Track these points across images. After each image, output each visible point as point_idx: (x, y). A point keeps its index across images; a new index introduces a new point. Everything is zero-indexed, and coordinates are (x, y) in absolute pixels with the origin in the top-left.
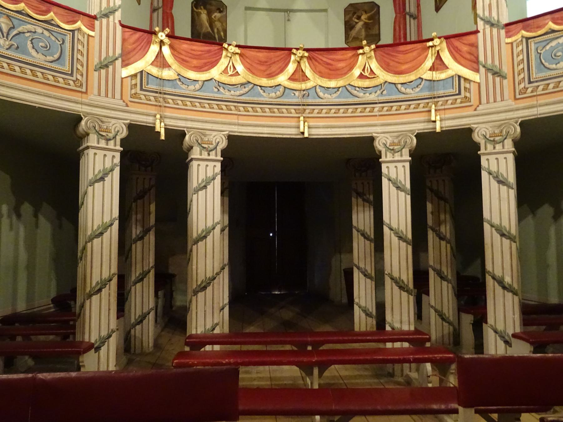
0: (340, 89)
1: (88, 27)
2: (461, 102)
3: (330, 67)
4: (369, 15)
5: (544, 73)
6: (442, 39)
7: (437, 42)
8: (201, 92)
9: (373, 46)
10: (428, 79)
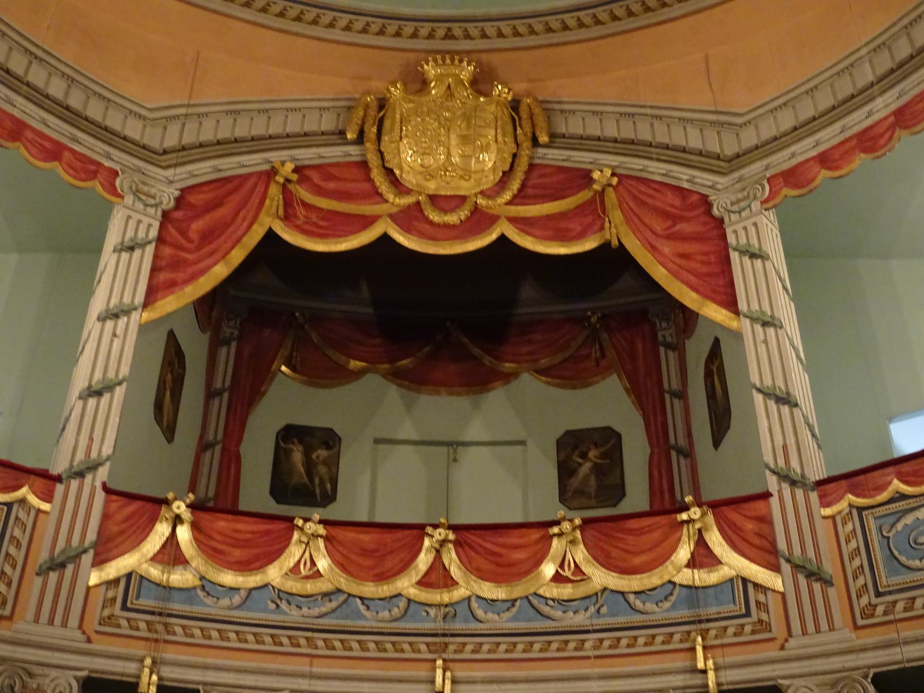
0: (518, 603)
1: (41, 495)
2: (753, 632)
3: (499, 559)
4: (603, 449)
5: (902, 577)
6: (705, 508)
7: (695, 512)
8: (243, 610)
9: (578, 522)
10: (685, 583)
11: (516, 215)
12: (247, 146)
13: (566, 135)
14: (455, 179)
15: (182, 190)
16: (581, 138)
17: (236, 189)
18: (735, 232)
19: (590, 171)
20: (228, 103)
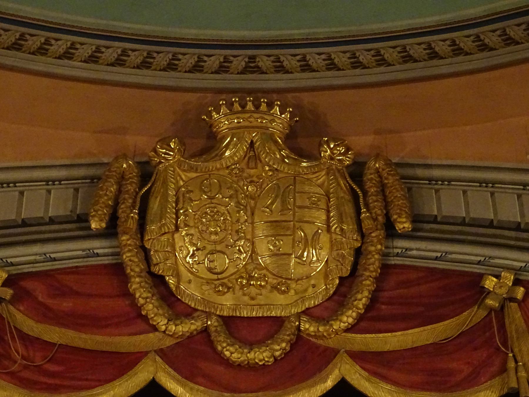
11: (364, 349)
14: (264, 291)
16: (463, 223)
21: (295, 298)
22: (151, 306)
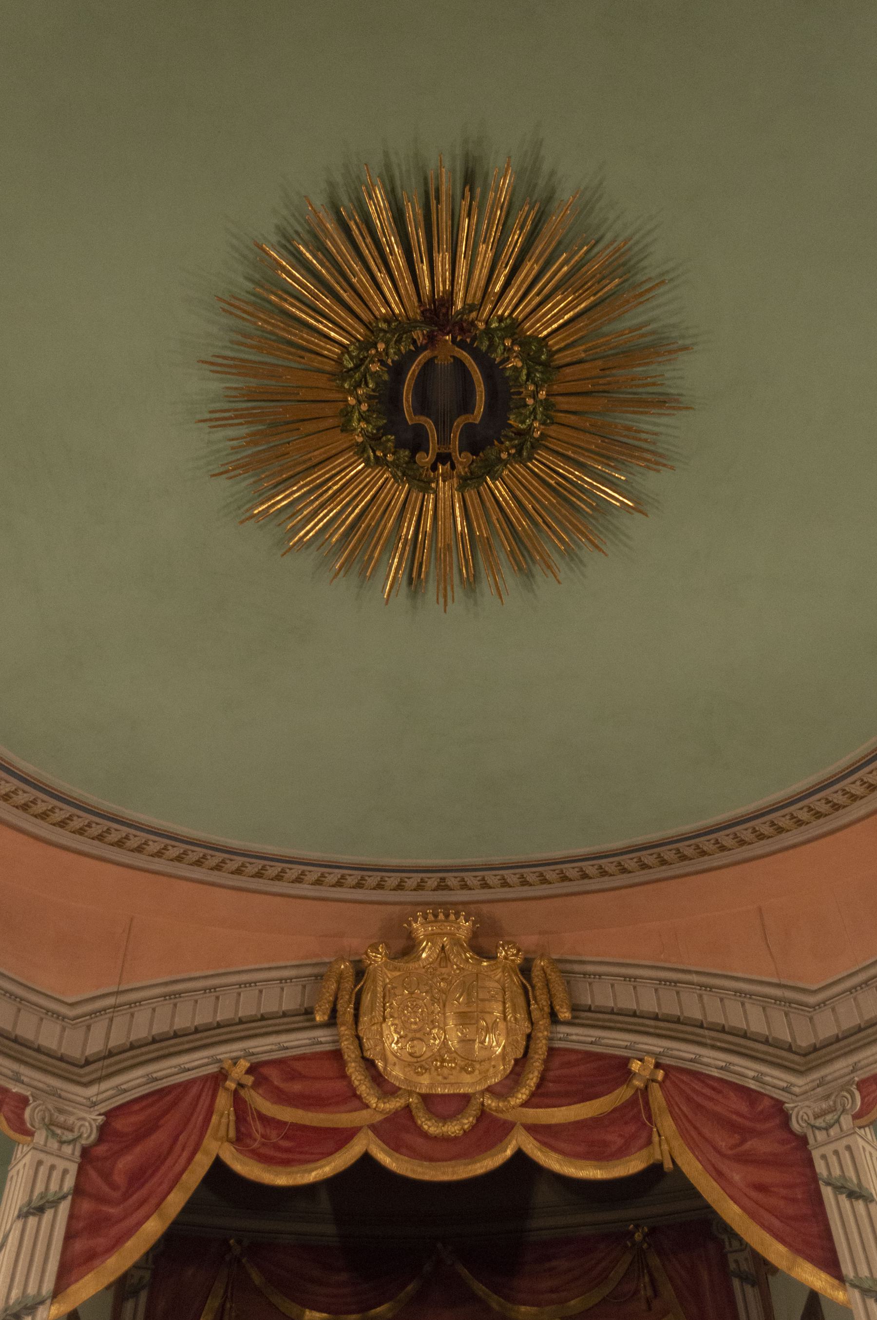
11: (536, 1122)
12: (188, 1042)
13: (593, 1008)
14: (454, 1072)
15: (108, 1114)
16: (612, 1012)
17: (174, 1104)
18: (824, 1157)
19: (625, 1062)
20: (166, 984)
21: (479, 1077)
22: (364, 1087)
